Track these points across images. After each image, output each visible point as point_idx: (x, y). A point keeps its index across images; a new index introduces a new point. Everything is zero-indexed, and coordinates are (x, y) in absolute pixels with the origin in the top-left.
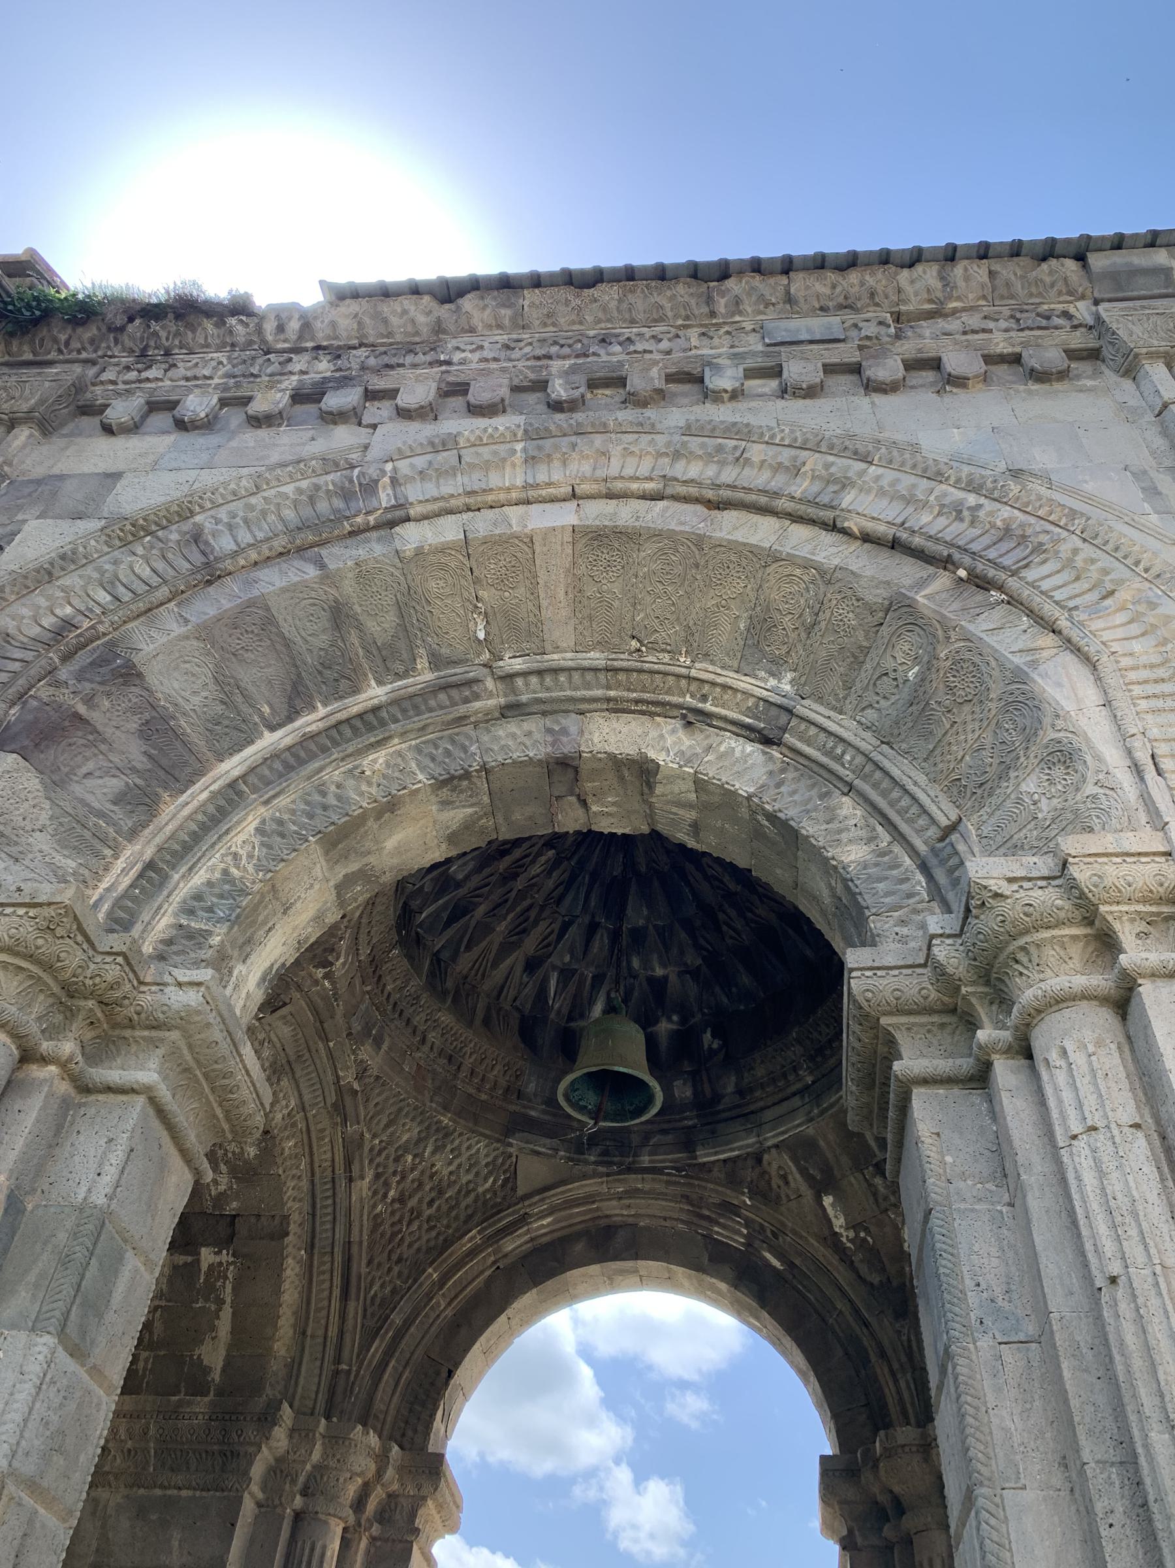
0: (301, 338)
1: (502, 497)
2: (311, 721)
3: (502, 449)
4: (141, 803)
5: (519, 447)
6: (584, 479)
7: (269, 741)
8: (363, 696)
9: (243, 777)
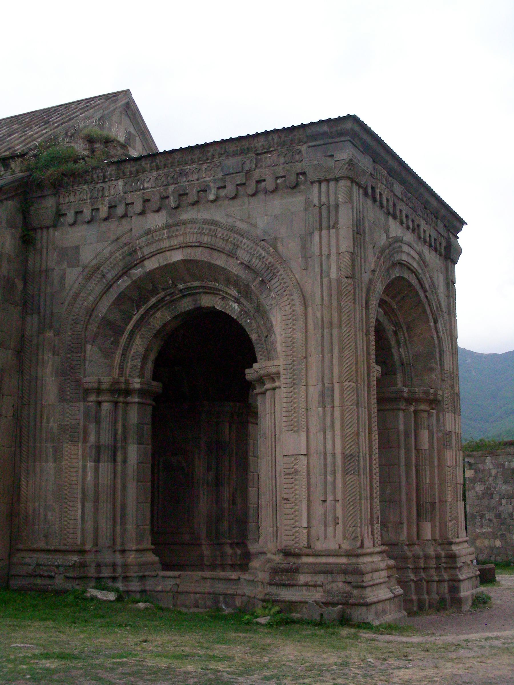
0: (104, 179)
1: (165, 250)
2: (142, 311)
3: (162, 232)
4: (116, 343)
5: (165, 231)
6: (182, 243)
7: (135, 318)
8: (151, 301)
9: (133, 328)
